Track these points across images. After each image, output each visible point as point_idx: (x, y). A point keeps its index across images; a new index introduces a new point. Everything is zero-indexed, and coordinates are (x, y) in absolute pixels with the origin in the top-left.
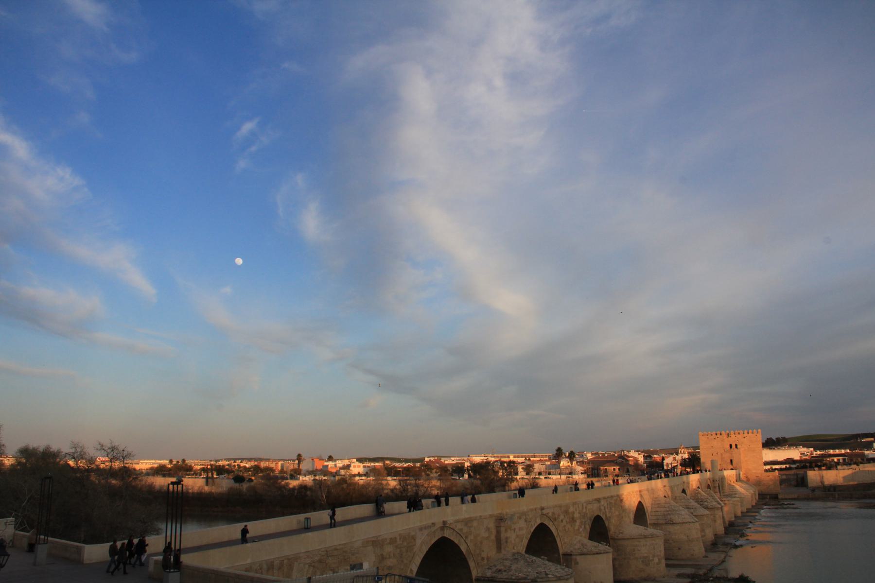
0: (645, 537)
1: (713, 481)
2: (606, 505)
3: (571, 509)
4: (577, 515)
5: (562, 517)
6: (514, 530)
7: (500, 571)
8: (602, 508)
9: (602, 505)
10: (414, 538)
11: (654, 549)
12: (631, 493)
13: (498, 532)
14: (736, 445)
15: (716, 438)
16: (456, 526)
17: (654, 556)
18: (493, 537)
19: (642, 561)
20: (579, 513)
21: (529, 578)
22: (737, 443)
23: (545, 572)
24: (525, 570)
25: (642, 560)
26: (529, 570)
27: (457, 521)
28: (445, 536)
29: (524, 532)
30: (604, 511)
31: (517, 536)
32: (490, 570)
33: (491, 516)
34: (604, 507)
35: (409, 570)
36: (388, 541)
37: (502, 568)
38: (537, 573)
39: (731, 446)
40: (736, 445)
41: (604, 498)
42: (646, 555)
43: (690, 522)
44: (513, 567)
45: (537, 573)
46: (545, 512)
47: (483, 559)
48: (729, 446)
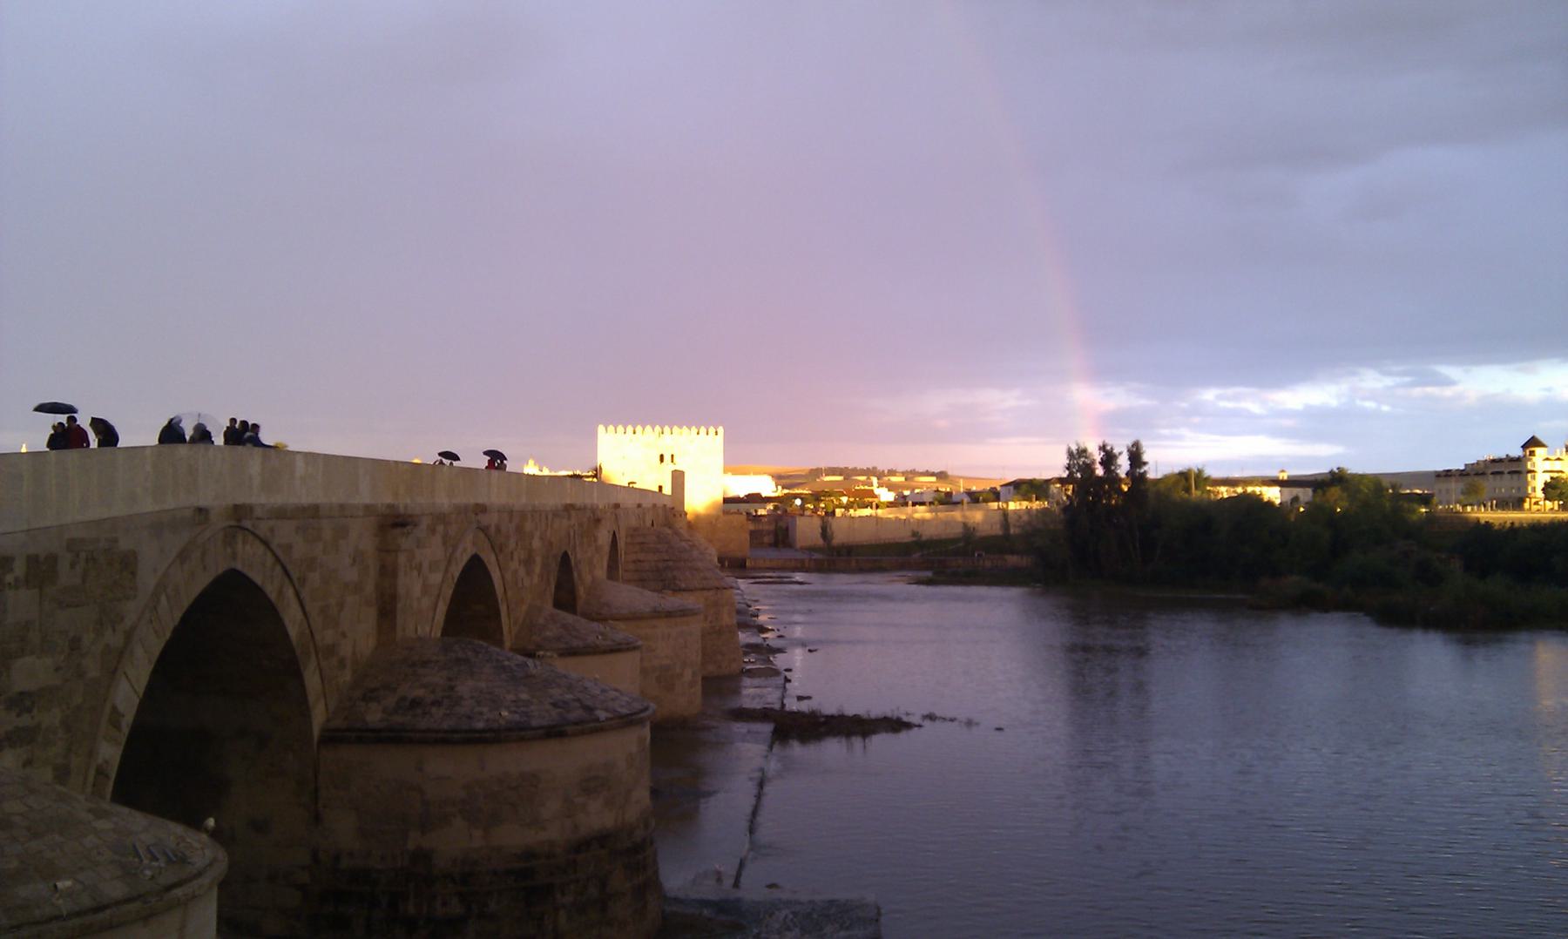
0: (669, 615)
3: (528, 526)
4: (536, 543)
5: (512, 543)
6: (419, 568)
7: (416, 703)
8: (572, 534)
10: (128, 562)
13: (388, 572)
16: (272, 530)
18: (369, 588)
20: (541, 538)
21: (534, 723)
23: (578, 700)
24: (511, 697)
26: (524, 696)
27: (281, 514)
28: (239, 567)
29: (436, 578)
31: (426, 589)
32: (373, 705)
33: (369, 509)
35: (108, 709)
36: (19, 569)
37: (420, 692)
38: (555, 705)
39: (662, 457)
43: (718, 588)
44: (465, 687)
45: (555, 705)
46: (485, 519)
47: (342, 663)
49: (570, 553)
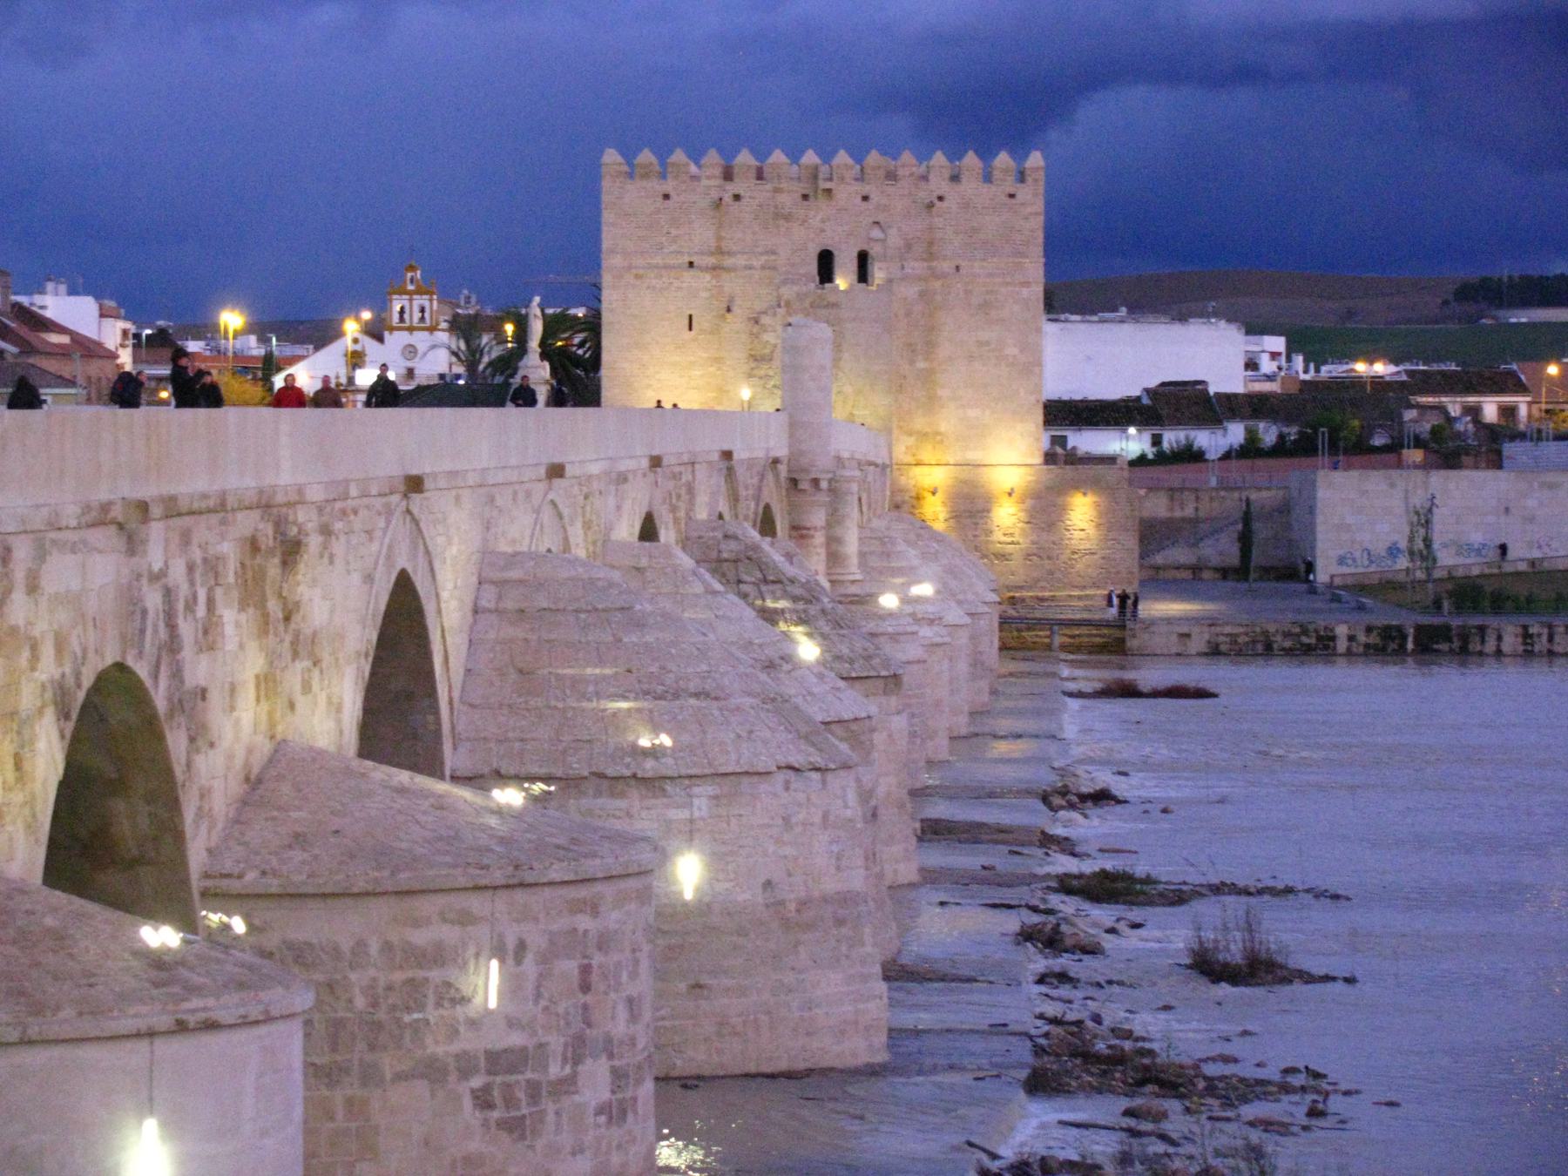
1: (794, 482)
2: (178, 572)
8: (153, 600)
9: (155, 577)
11: (586, 987)
12: (354, 492)
14: (863, 259)
15: (727, 198)
17: (577, 1051)
19: (483, 1100)
22: (875, 250)
25: (477, 1082)
30: (163, 633)
34: (168, 593)
39: (826, 266)
40: (863, 259)
41: (172, 508)
42: (516, 1039)
48: (813, 268)
49: (142, 670)
